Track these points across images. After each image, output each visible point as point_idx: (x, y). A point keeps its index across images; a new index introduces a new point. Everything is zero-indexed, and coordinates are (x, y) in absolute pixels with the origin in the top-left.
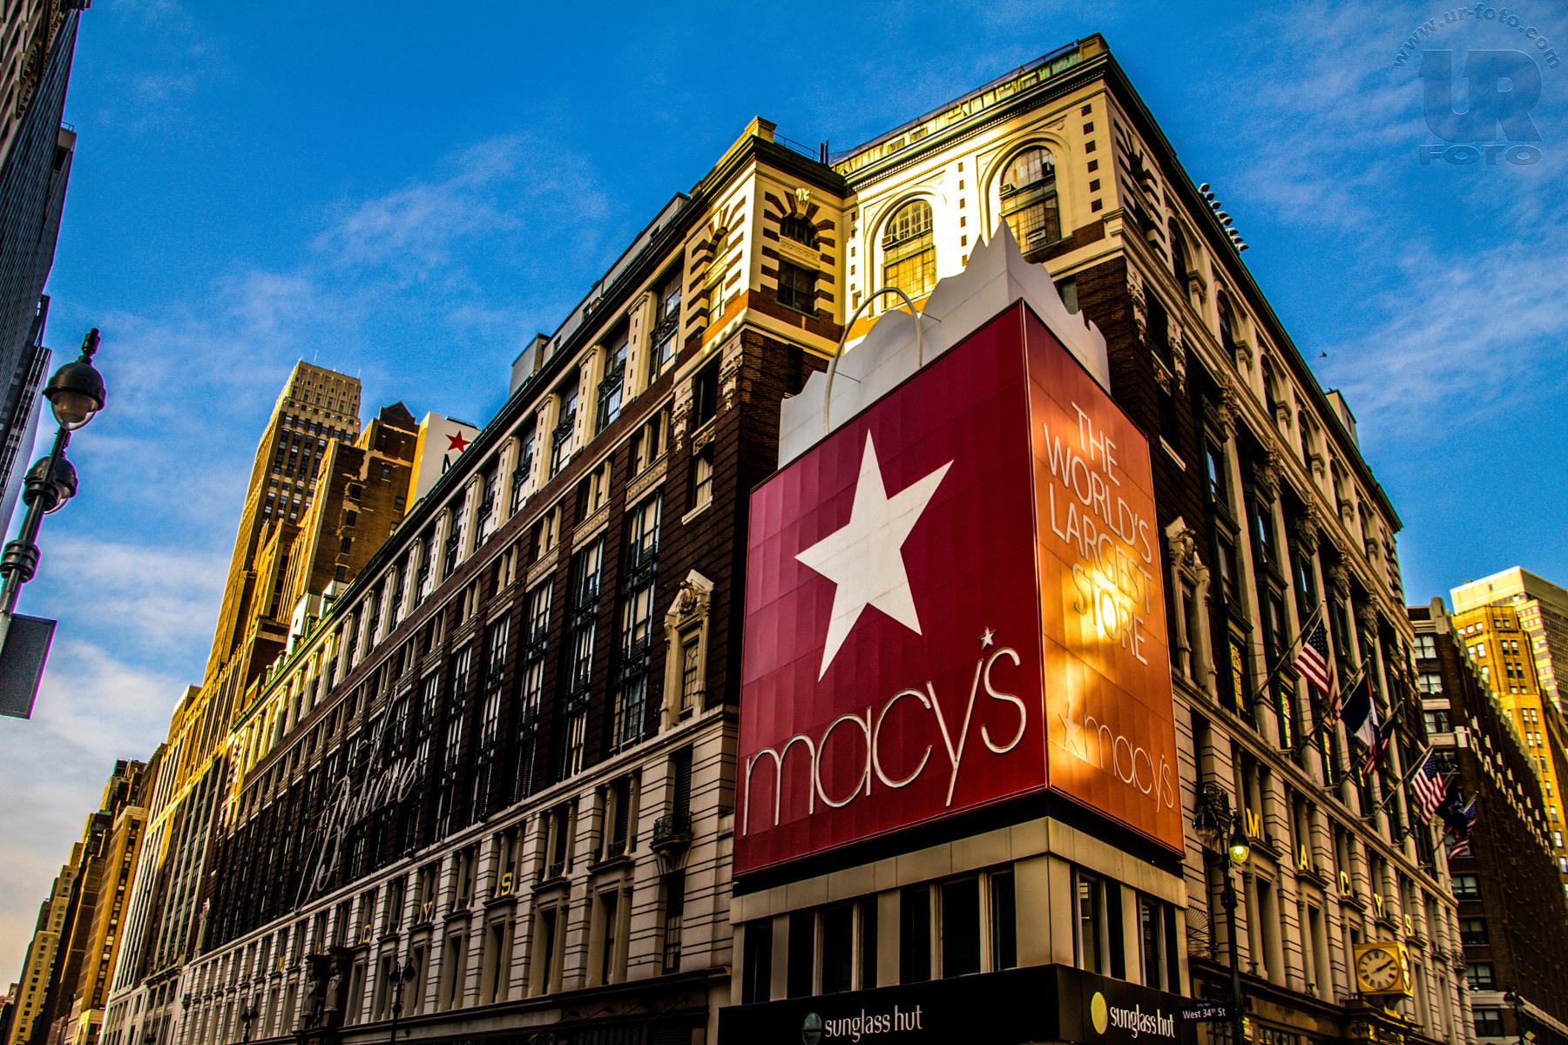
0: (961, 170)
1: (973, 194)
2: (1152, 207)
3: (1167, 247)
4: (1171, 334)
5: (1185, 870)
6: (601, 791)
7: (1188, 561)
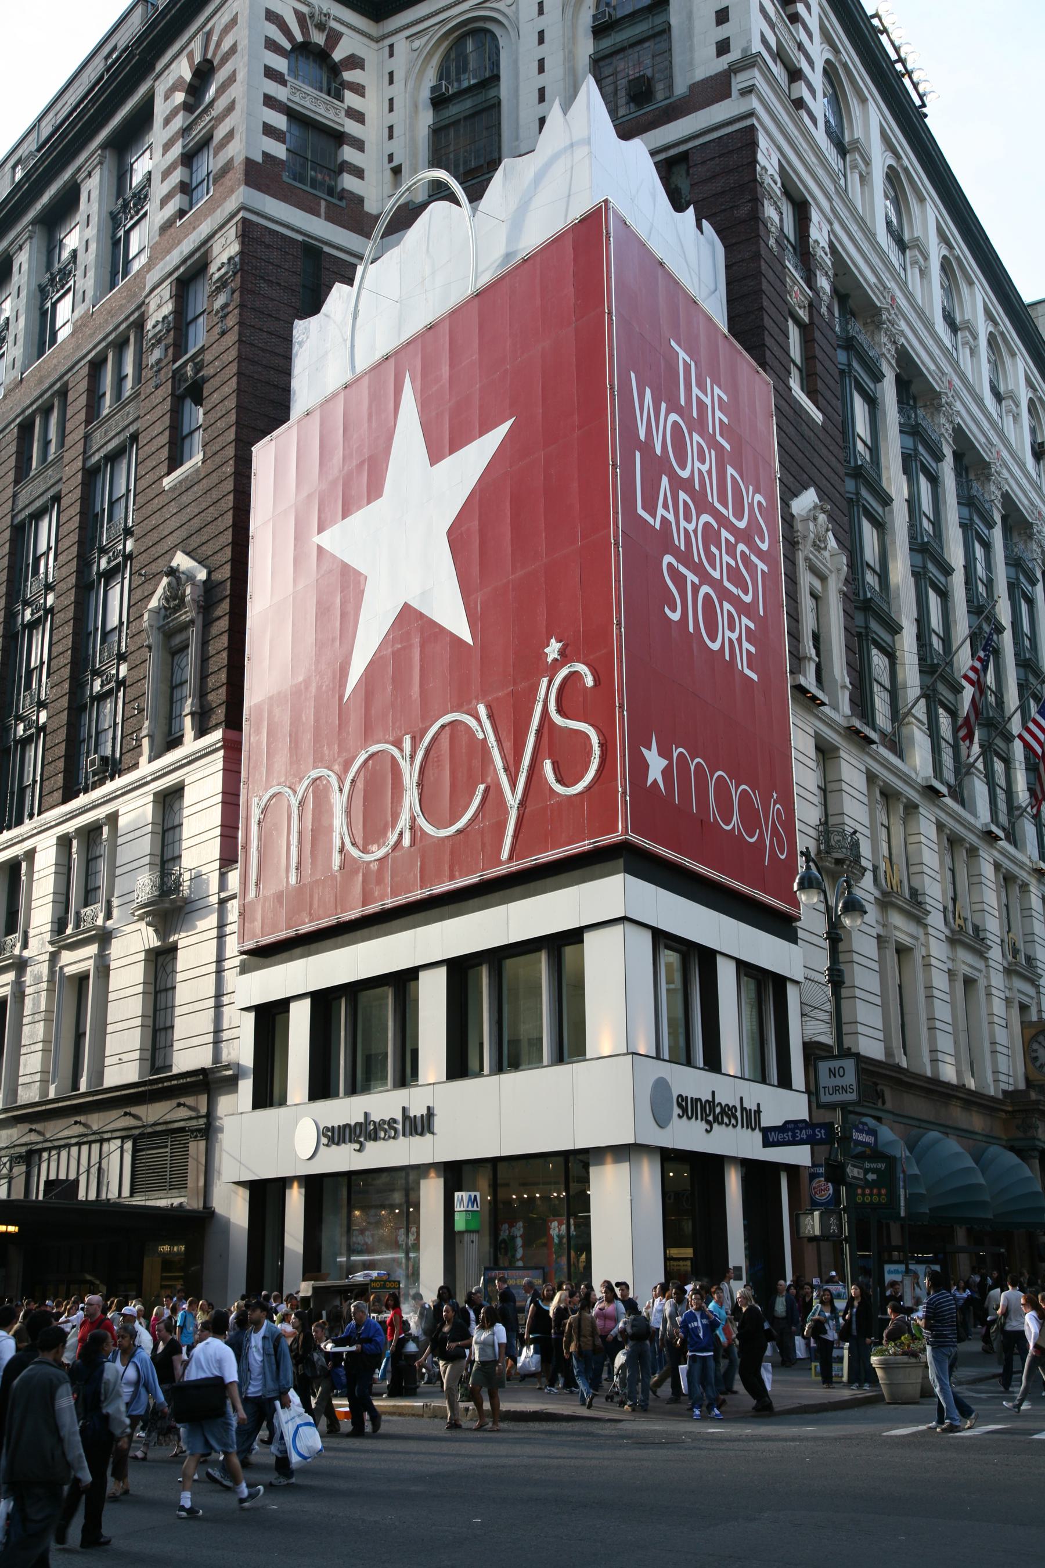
2: (800, 46)
3: (819, 106)
4: (814, 233)
5: (801, 933)
6: (64, 842)
7: (819, 546)
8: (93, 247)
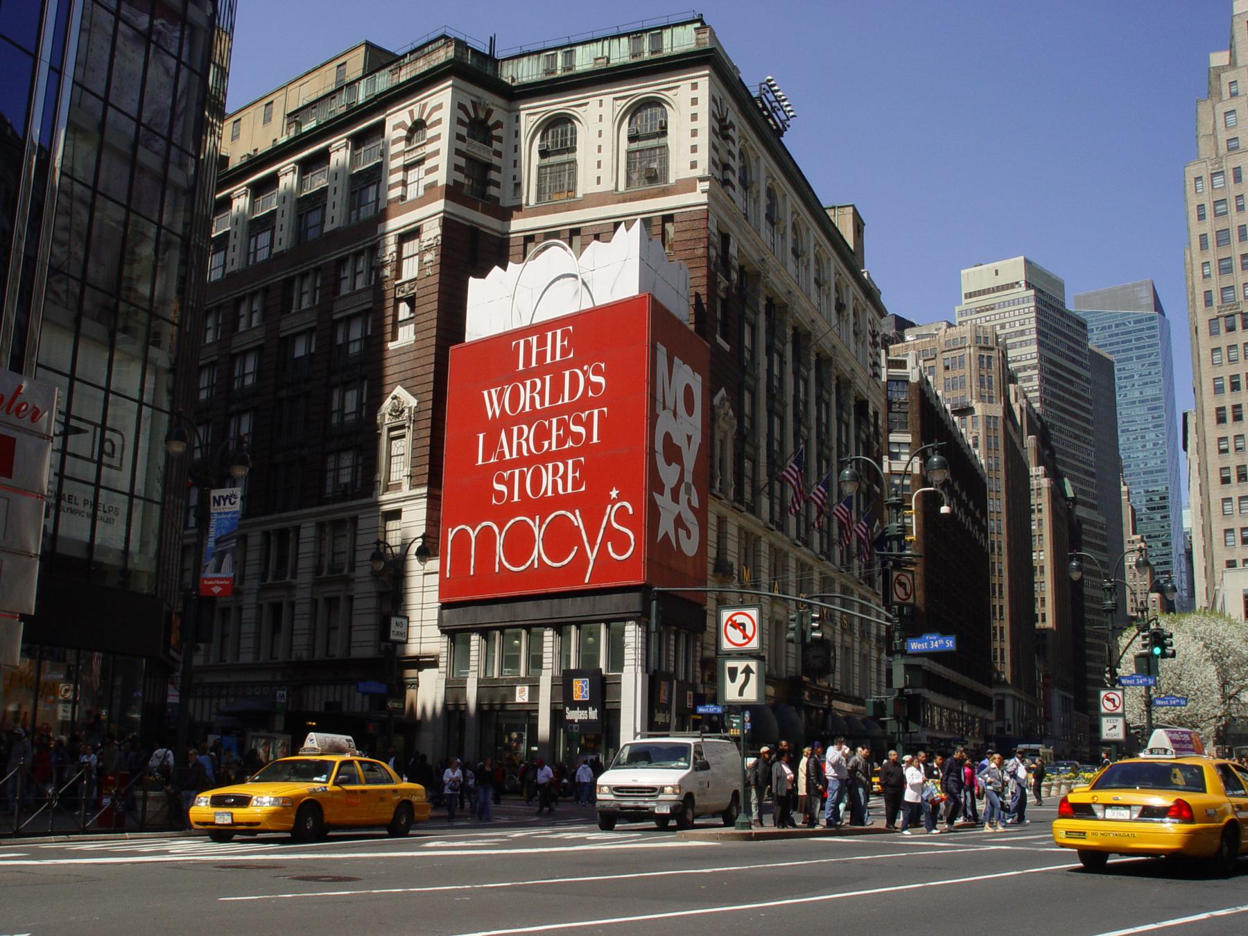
0: (601, 105)
1: (608, 127)
8: (339, 192)
